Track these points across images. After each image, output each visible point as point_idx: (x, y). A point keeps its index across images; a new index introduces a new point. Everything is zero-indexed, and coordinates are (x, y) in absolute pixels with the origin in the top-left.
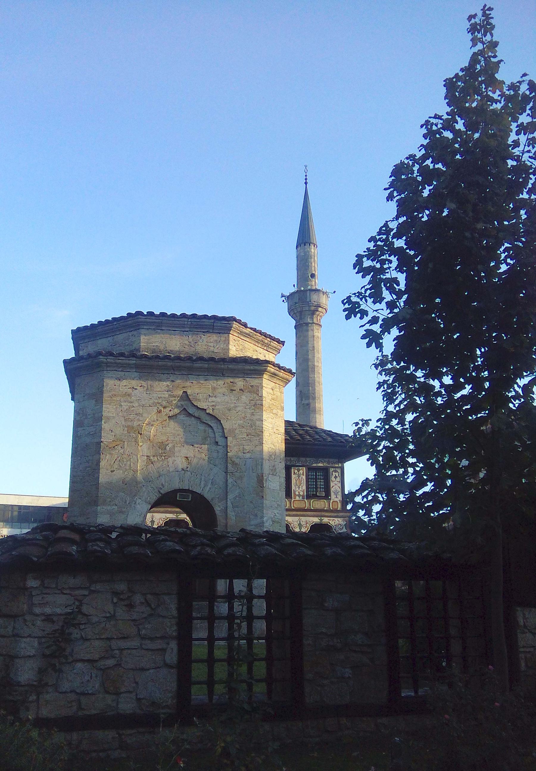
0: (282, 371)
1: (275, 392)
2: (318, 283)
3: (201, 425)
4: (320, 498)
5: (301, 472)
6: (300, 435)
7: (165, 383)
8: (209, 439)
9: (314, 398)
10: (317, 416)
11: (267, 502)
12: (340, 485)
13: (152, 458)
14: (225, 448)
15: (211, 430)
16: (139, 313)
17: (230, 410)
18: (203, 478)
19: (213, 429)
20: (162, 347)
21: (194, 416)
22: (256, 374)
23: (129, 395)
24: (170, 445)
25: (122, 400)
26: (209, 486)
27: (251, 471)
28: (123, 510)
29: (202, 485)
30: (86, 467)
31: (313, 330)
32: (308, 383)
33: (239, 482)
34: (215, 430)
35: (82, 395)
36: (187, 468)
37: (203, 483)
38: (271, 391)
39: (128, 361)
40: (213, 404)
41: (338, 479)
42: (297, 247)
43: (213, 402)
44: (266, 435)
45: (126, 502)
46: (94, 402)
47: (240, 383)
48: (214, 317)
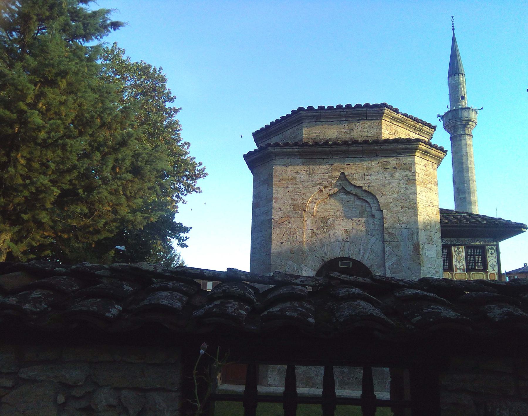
0: (434, 149)
1: (428, 169)
2: (468, 103)
3: (359, 201)
4: (479, 271)
5: (461, 249)
6: (458, 220)
7: (324, 167)
8: (366, 213)
9: (469, 193)
10: (473, 207)
11: (425, 268)
12: (496, 260)
15: (367, 205)
16: (301, 109)
17: (384, 186)
18: (362, 247)
19: (369, 204)
20: (321, 136)
22: (407, 152)
23: (295, 178)
24: (331, 220)
25: (289, 182)
31: (465, 140)
32: (464, 182)
37: (361, 252)
38: (424, 168)
39: (291, 150)
41: (494, 255)
42: (448, 78)
43: (368, 180)
45: (294, 269)
47: (393, 162)
48: (367, 106)
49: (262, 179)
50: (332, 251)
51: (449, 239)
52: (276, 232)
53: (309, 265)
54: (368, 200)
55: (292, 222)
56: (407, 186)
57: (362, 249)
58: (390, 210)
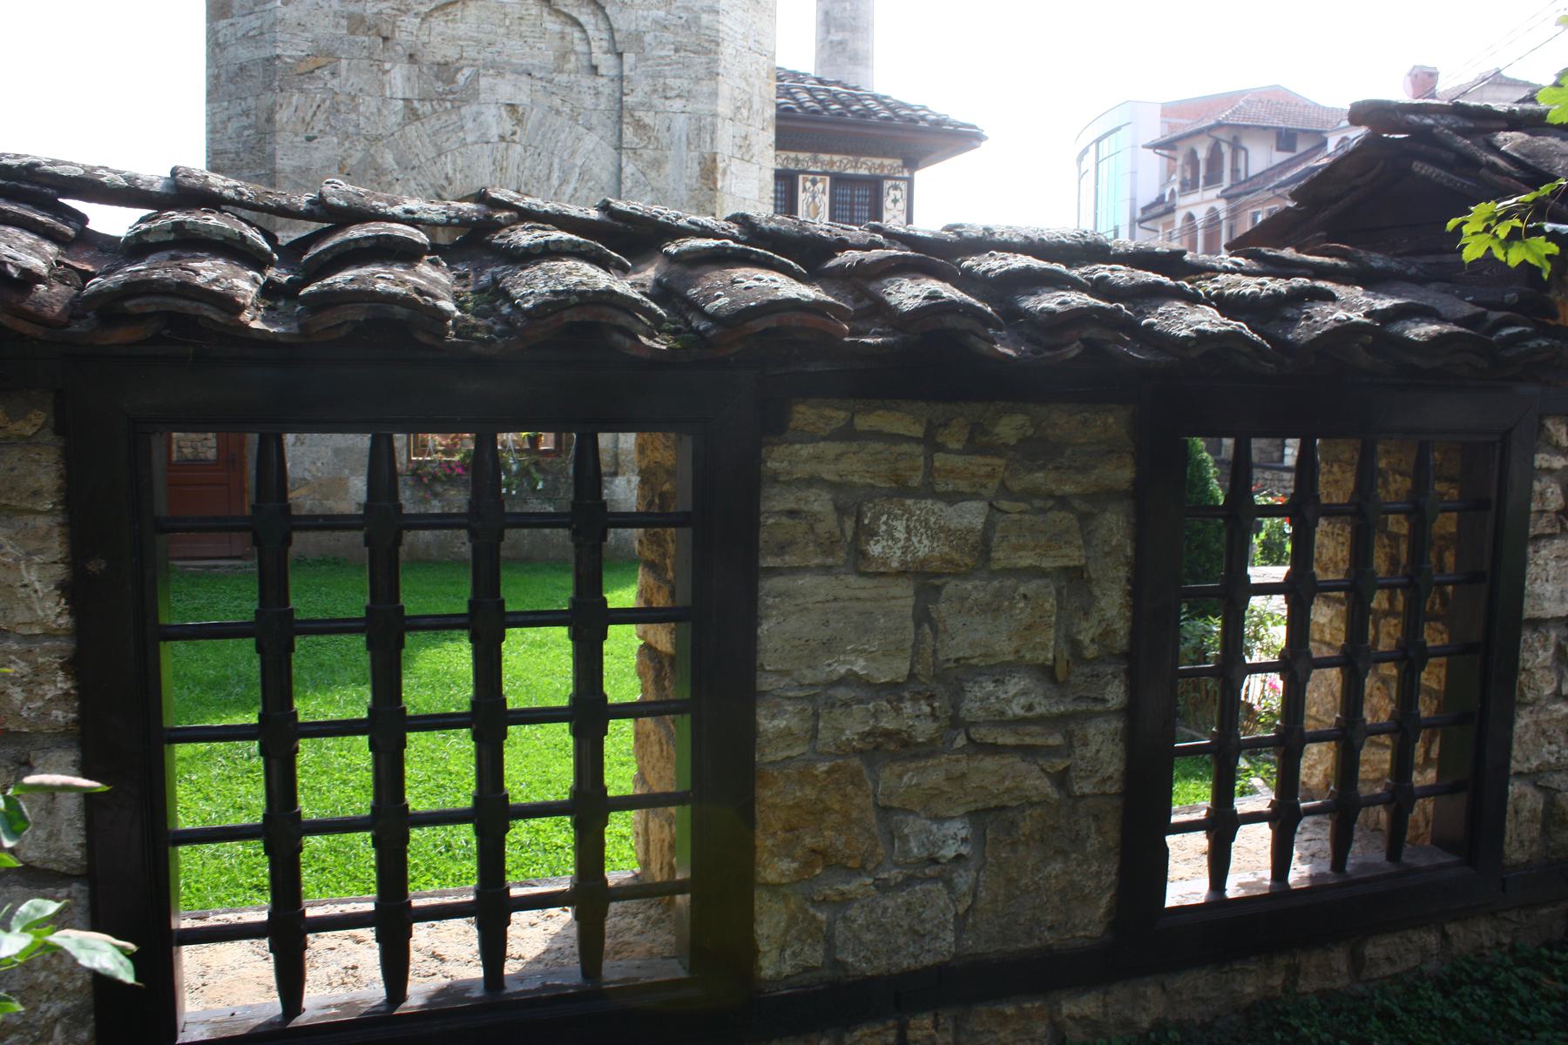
5: (820, 186)
6: (820, 102)
8: (573, 58)
9: (854, 30)
13: (416, 104)
14: (616, 85)
15: (577, 35)
18: (556, 160)
19: (584, 31)
24: (467, 72)
26: (573, 184)
27: (684, 147)
29: (555, 182)
30: (245, 128)
33: (653, 174)
34: (590, 32)
36: (514, 133)
41: (902, 205)
44: (727, 51)
50: (467, 171)
51: (792, 155)
52: (290, 104)
54: (582, 19)
55: (344, 73)
57: (556, 166)
58: (642, 56)
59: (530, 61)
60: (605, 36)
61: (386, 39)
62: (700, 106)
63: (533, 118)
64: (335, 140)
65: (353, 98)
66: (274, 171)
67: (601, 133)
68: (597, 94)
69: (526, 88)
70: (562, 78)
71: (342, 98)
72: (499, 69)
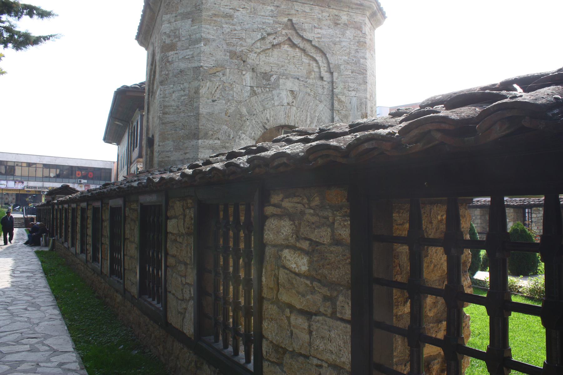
3: (306, 58)
7: (269, 8)
8: (313, 74)
13: (255, 88)
14: (330, 85)
15: (315, 64)
17: (335, 44)
18: (309, 114)
21: (299, 48)
23: (231, 17)
24: (275, 77)
25: (223, 20)
27: (356, 111)
28: (227, 145)
29: (308, 123)
30: (182, 96)
34: (320, 64)
35: (174, 15)
36: (293, 102)
37: (309, 120)
40: (320, 36)
43: (318, 33)
45: (229, 136)
46: (189, 22)
49: (179, 11)
50: (275, 117)
52: (206, 86)
53: (248, 133)
54: (317, 58)
55: (228, 74)
56: (357, 48)
57: (308, 116)
59: (297, 74)
60: (326, 65)
61: (244, 61)
62: (361, 94)
63: (300, 96)
64: (224, 102)
65: (231, 85)
66: (198, 114)
67: (325, 103)
68: (323, 88)
69: (297, 84)
70: (310, 81)
71: (226, 84)
72: (287, 77)
